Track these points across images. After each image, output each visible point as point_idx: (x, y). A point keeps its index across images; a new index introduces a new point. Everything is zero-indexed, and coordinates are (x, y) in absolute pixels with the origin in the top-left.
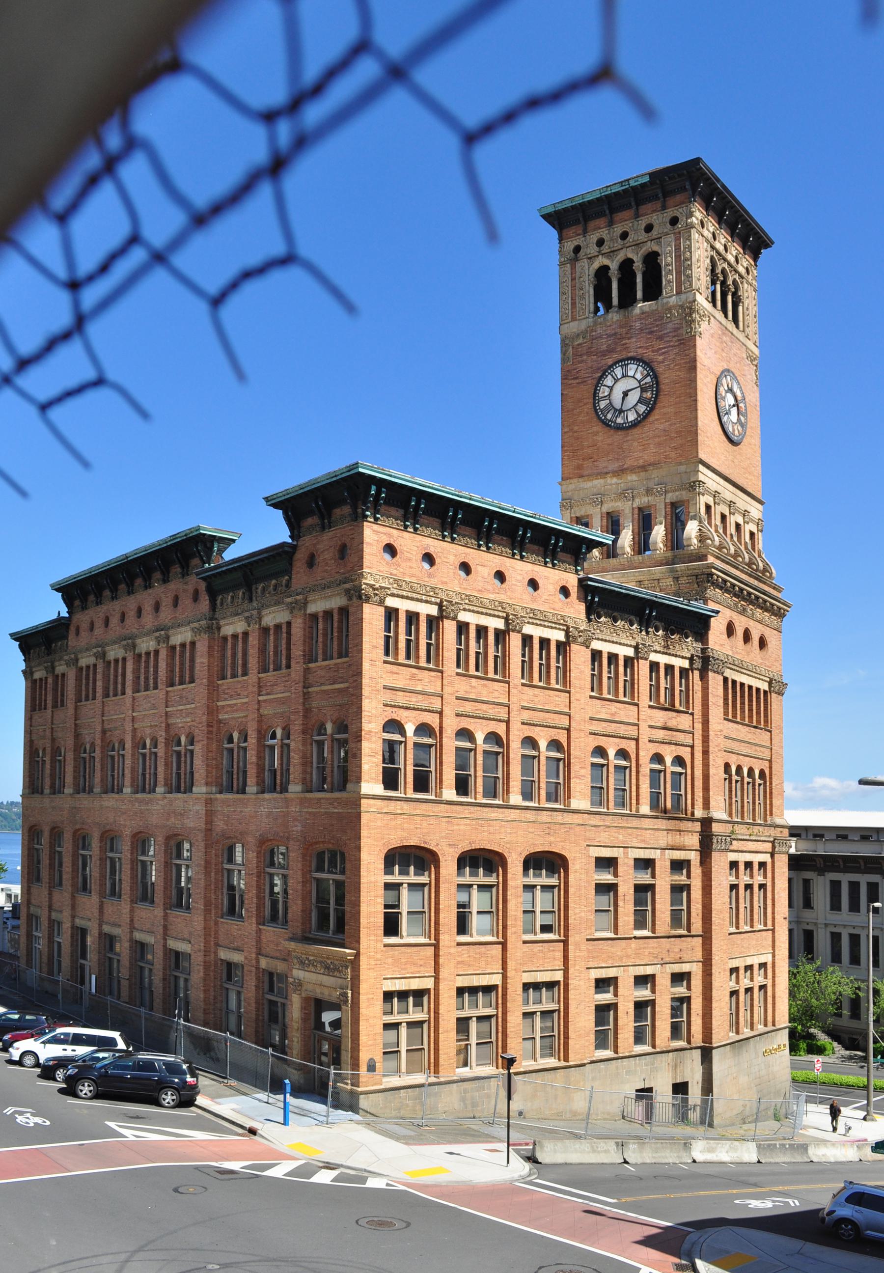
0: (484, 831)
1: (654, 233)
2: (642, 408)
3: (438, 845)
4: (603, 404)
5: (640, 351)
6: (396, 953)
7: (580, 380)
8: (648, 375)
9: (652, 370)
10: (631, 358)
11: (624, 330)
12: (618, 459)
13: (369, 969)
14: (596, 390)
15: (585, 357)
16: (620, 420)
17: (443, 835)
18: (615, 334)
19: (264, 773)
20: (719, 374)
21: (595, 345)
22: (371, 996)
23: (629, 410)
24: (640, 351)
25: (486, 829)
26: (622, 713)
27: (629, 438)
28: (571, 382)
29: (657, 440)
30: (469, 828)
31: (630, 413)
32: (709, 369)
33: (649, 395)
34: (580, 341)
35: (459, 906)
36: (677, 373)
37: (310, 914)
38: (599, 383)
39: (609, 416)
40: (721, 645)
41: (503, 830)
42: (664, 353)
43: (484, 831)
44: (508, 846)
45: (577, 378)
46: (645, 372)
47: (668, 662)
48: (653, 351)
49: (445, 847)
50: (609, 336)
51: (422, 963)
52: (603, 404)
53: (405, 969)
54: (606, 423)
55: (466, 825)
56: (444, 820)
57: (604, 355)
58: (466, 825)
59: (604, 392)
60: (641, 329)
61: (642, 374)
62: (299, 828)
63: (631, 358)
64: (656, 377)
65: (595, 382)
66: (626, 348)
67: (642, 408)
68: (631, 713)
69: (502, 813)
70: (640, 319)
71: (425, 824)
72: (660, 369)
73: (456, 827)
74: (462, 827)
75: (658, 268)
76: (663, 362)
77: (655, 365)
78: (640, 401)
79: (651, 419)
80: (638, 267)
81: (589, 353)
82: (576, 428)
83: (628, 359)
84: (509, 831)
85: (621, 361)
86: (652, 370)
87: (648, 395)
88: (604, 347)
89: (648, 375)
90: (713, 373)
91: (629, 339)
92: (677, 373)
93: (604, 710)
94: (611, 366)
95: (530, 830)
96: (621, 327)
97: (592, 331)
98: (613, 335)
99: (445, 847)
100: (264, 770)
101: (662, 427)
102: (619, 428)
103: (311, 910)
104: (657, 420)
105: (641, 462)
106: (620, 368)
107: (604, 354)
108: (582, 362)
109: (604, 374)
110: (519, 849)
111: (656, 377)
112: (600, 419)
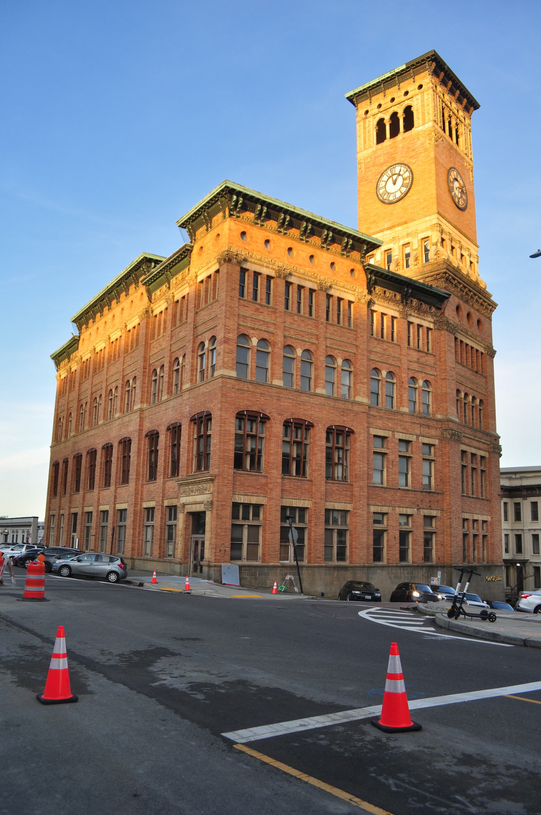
0: (301, 408)
1: (409, 96)
2: (404, 190)
3: (271, 413)
4: (381, 191)
5: (402, 159)
6: (242, 478)
8: (407, 171)
9: (409, 167)
10: (397, 164)
11: (393, 150)
13: (224, 485)
14: (377, 184)
15: (371, 168)
16: (391, 198)
17: (275, 407)
18: (388, 152)
19: (172, 387)
20: (448, 169)
22: (224, 503)
25: (302, 407)
26: (391, 349)
27: (397, 207)
30: (291, 405)
32: (442, 165)
33: (407, 181)
34: (369, 160)
35: (284, 455)
36: (424, 167)
37: (192, 461)
38: (379, 180)
39: (385, 197)
40: (453, 318)
41: (313, 409)
43: (301, 408)
44: (316, 419)
46: (405, 170)
47: (419, 323)
48: (410, 158)
49: (275, 415)
50: (384, 154)
51: (259, 487)
53: (248, 490)
54: (383, 202)
55: (289, 403)
56: (275, 398)
58: (289, 403)
59: (382, 184)
60: (403, 147)
62: (188, 409)
63: (397, 164)
64: (412, 172)
66: (394, 159)
68: (396, 350)
69: (313, 398)
70: (402, 142)
71: (262, 399)
72: (413, 167)
73: (282, 403)
74: (286, 404)
75: (412, 113)
78: (402, 186)
79: (409, 194)
80: (401, 116)
81: (373, 166)
82: (366, 207)
84: (317, 410)
86: (409, 167)
87: (407, 181)
89: (407, 171)
90: (445, 167)
91: (396, 154)
92: (424, 167)
93: (379, 346)
94: (386, 170)
95: (331, 411)
96: (392, 148)
97: (375, 153)
99: (275, 415)
100: (172, 385)
101: (415, 198)
102: (391, 203)
103: (192, 459)
104: (413, 194)
105: (404, 220)
107: (382, 165)
108: (370, 171)
109: (382, 175)
110: (324, 422)
111: (412, 172)
112: (380, 200)
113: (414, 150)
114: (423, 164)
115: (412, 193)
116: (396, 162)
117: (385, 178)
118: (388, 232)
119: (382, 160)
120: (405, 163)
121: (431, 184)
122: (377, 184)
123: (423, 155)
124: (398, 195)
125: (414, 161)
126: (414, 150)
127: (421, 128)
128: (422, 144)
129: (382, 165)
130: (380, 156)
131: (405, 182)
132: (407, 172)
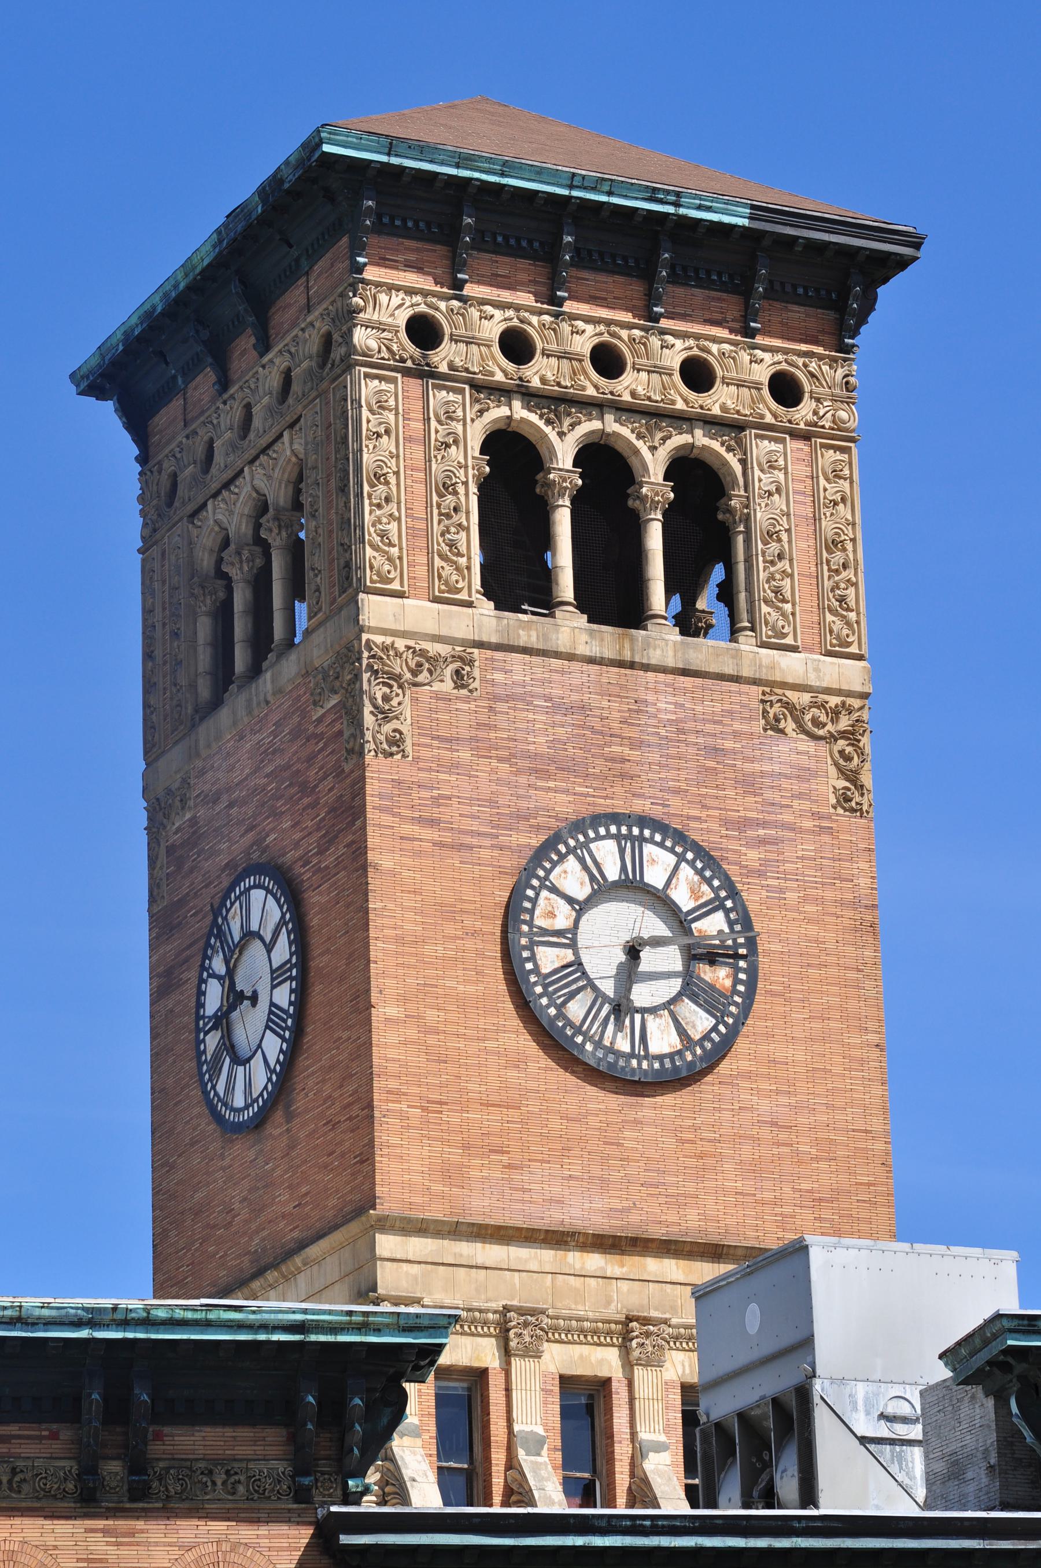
5: (676, 803)
7: (447, 838)
8: (715, 905)
12: (604, 1183)
18: (583, 708)
21: (501, 721)
23: (653, 1010)
24: (676, 803)
28: (408, 829)
29: (747, 1150)
31: (653, 1024)
33: (720, 976)
42: (763, 842)
45: (433, 823)
48: (726, 823)
50: (556, 707)
52: (549, 958)
57: (547, 775)
61: (694, 893)
65: (513, 862)
66: (622, 773)
67: (699, 1021)
72: (753, 898)
76: (761, 874)
77: (732, 870)
81: (482, 748)
83: (643, 821)
85: (615, 818)
88: (540, 743)
91: (636, 744)
92: (813, 930)
94: (578, 826)
98: (570, 710)
101: (764, 1106)
104: (748, 1076)
106: (611, 845)
107: (541, 768)
108: (453, 767)
113: (749, 784)
114: (810, 908)
115: (744, 1065)
116: (641, 806)
117: (570, 876)
118: (594, 1261)
119: (539, 732)
120: (694, 836)
121: (862, 1061)
122: (516, 895)
123: (807, 848)
124: (662, 1039)
125: (753, 856)
126: (749, 784)
127: (791, 666)
128: (804, 775)
129: (541, 768)
130: (527, 699)
131: (707, 973)
132: (720, 915)
